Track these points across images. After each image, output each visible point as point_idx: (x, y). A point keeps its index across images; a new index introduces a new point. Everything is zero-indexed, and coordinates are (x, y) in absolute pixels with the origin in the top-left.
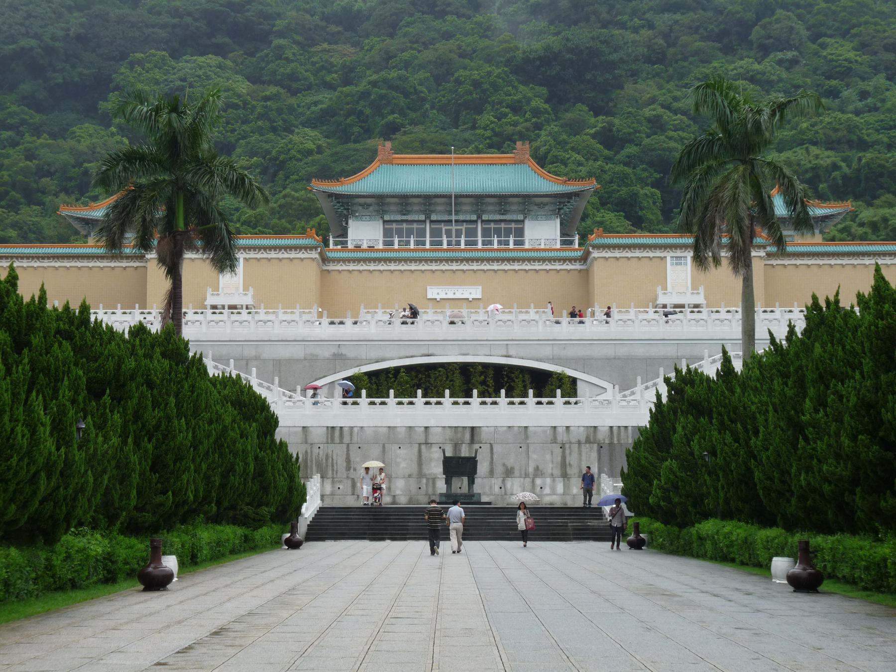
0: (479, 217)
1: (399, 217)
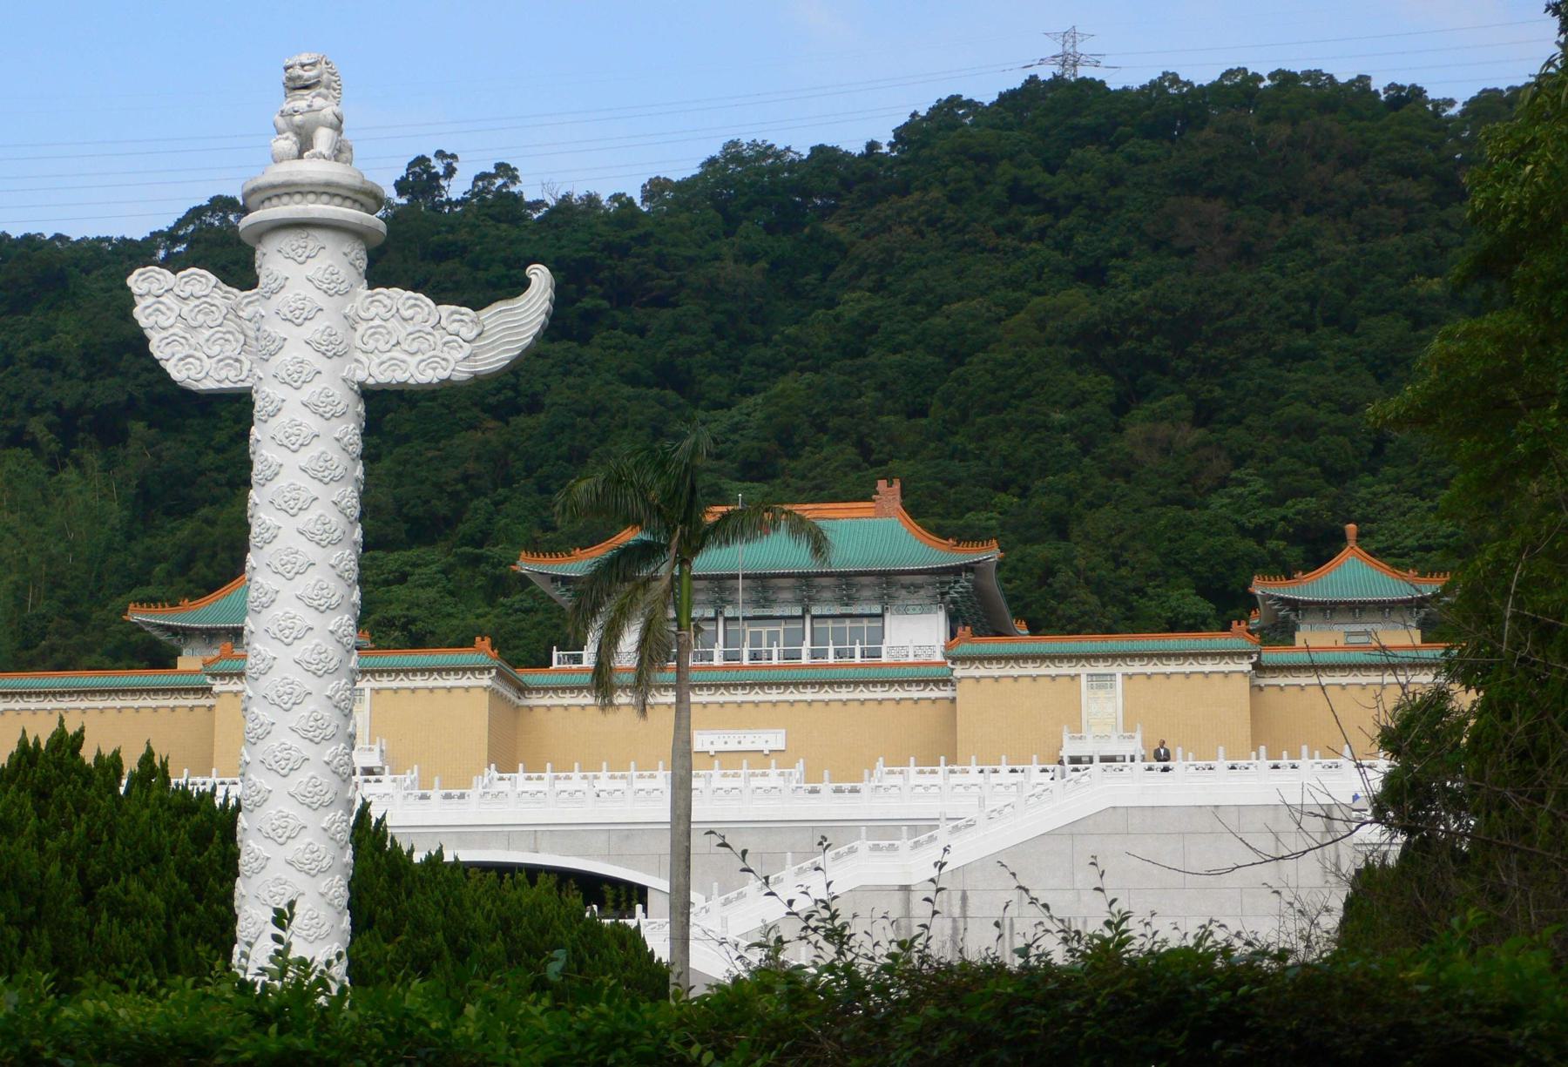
0: (806, 610)
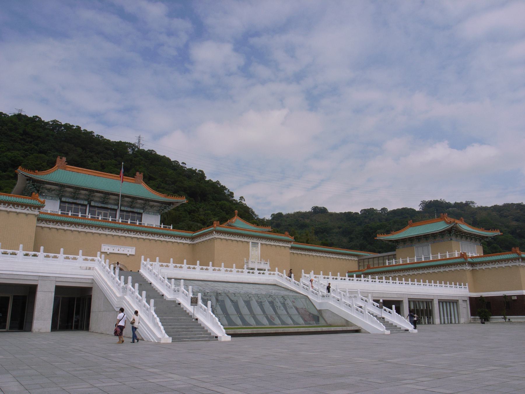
1: (71, 200)
